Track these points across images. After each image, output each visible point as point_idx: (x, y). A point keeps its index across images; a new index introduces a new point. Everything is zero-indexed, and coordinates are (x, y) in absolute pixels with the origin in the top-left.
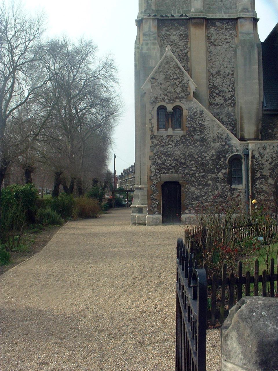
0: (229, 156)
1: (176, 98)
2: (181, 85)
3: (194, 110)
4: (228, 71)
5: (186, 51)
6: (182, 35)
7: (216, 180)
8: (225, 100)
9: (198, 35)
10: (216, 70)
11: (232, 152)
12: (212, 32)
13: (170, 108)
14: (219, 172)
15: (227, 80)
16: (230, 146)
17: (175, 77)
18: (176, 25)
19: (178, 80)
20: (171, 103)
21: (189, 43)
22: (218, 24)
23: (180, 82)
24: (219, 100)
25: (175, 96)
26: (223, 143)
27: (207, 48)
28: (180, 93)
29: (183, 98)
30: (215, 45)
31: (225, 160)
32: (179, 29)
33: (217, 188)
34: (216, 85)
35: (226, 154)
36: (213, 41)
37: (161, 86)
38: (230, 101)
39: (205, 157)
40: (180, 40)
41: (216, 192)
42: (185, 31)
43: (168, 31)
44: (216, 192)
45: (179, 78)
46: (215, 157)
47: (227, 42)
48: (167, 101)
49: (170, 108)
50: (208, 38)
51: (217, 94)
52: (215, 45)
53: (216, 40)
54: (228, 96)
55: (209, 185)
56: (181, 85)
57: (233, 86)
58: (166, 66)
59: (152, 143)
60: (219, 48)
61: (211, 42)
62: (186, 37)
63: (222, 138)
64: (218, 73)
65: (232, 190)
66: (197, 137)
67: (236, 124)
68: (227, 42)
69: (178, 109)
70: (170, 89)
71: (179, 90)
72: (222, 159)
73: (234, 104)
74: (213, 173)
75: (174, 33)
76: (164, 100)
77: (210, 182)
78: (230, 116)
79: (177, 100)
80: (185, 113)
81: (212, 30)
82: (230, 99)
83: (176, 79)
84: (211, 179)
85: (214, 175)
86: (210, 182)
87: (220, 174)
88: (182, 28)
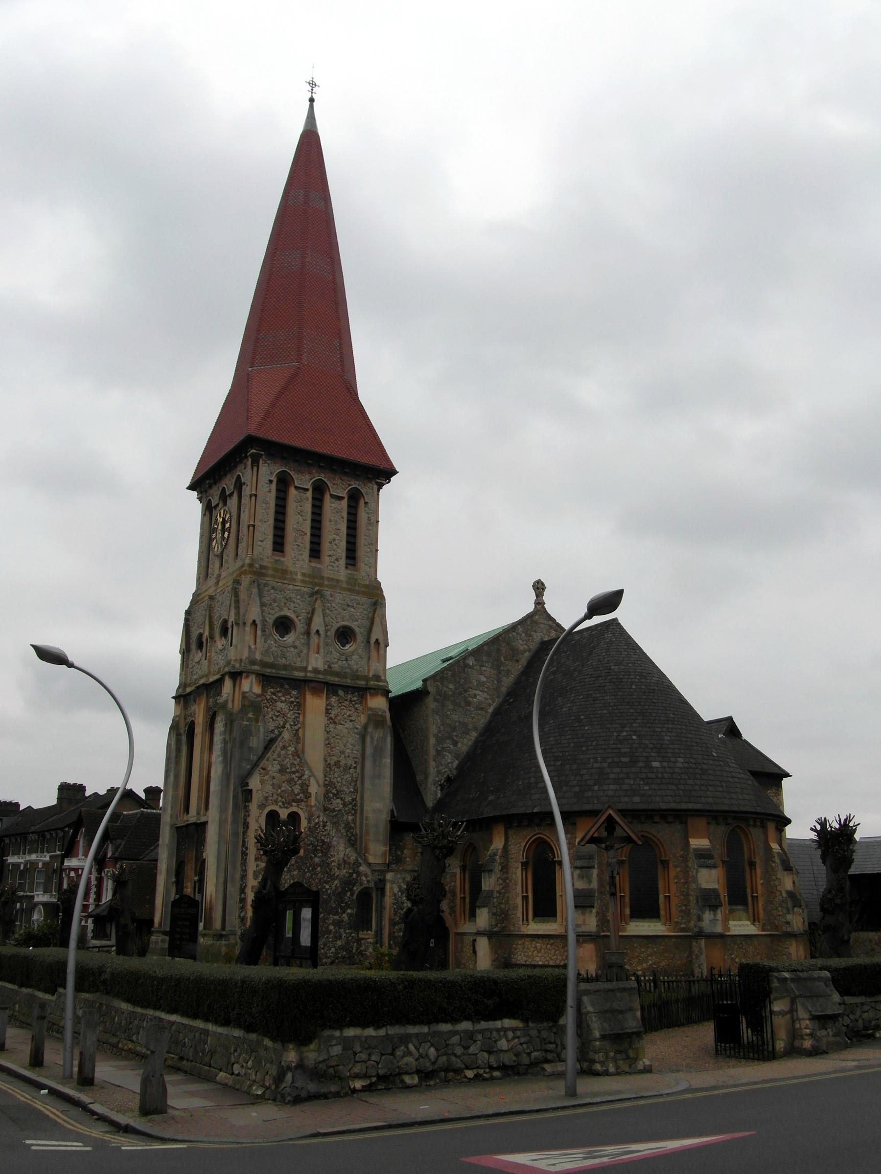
0: (357, 889)
1: (294, 801)
2: (300, 781)
3: (317, 821)
4: (350, 762)
5: (296, 727)
6: (292, 702)
7: (338, 924)
8: (344, 805)
9: (315, 705)
10: (335, 758)
11: (361, 884)
12: (333, 704)
13: (284, 814)
14: (344, 912)
15: (348, 776)
16: (359, 874)
17: (294, 769)
18: (287, 686)
19: (297, 774)
20: (287, 808)
21: (301, 716)
22: (341, 693)
23: (300, 778)
24: (337, 803)
25: (290, 798)
26: (351, 871)
27: (326, 726)
28: (298, 794)
29: (302, 801)
30: (335, 723)
31: (352, 894)
32: (289, 694)
33: (340, 937)
34: (335, 780)
35: (354, 885)
36: (332, 716)
37: (274, 781)
38: (350, 806)
39: (327, 890)
40: (290, 710)
41: (339, 943)
42: (297, 698)
43: (274, 694)
44: (339, 943)
45: (298, 771)
46: (340, 890)
47: (351, 721)
48: (280, 804)
49: (284, 814)
50: (327, 711)
51: (334, 795)
52: (335, 723)
53: (338, 715)
54: (348, 799)
55: (330, 932)
56: (300, 781)
57: (356, 785)
58: (283, 752)
59: (257, 866)
60: (339, 727)
61: (331, 718)
62: (299, 706)
63: (349, 863)
64: (337, 764)
65: (359, 941)
66: (317, 860)
67: (356, 840)
68: (351, 721)
69: (294, 818)
70: (285, 787)
71: (297, 789)
72: (348, 894)
73: (356, 811)
74: (336, 913)
75: (283, 699)
76: (276, 802)
77: (331, 927)
78: (351, 828)
79: (294, 804)
80: (304, 823)
81: (333, 699)
82: (351, 803)
83: (294, 773)
84: (334, 924)
85: (337, 917)
86: (331, 927)
87: (344, 915)
88: (294, 693)
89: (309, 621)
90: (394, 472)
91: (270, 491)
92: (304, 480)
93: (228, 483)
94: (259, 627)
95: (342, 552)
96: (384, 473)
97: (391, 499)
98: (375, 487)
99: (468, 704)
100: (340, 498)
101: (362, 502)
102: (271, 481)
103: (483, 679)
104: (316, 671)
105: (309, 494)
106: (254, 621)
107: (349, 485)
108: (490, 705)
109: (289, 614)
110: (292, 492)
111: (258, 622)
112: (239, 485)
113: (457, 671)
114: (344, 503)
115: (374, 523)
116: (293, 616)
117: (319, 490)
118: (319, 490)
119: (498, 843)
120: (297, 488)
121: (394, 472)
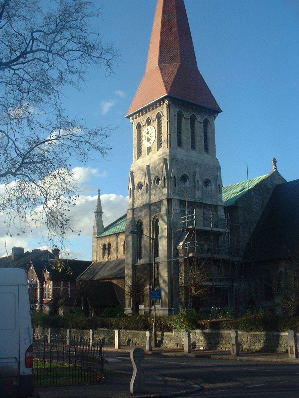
22: (208, 207)
89: (194, 176)
90: (219, 111)
91: (175, 119)
92: (187, 115)
93: (152, 115)
94: (177, 179)
95: (203, 146)
96: (215, 110)
97: (219, 122)
98: (213, 118)
99: (253, 211)
100: (201, 123)
101: (209, 124)
102: (175, 115)
103: (257, 201)
104: (199, 199)
105: (189, 121)
106: (175, 177)
107: (204, 117)
108: (260, 212)
109: (186, 173)
110: (183, 120)
111: (176, 177)
112: (159, 117)
113: (247, 197)
114: (202, 125)
115: (213, 133)
116: (188, 174)
117: (193, 120)
118: (193, 120)
119: (282, 269)
120: (185, 118)
121: (219, 111)
